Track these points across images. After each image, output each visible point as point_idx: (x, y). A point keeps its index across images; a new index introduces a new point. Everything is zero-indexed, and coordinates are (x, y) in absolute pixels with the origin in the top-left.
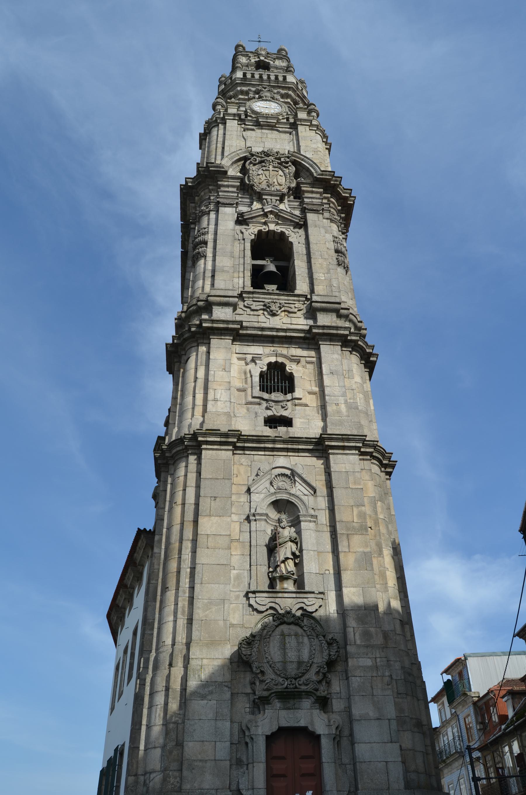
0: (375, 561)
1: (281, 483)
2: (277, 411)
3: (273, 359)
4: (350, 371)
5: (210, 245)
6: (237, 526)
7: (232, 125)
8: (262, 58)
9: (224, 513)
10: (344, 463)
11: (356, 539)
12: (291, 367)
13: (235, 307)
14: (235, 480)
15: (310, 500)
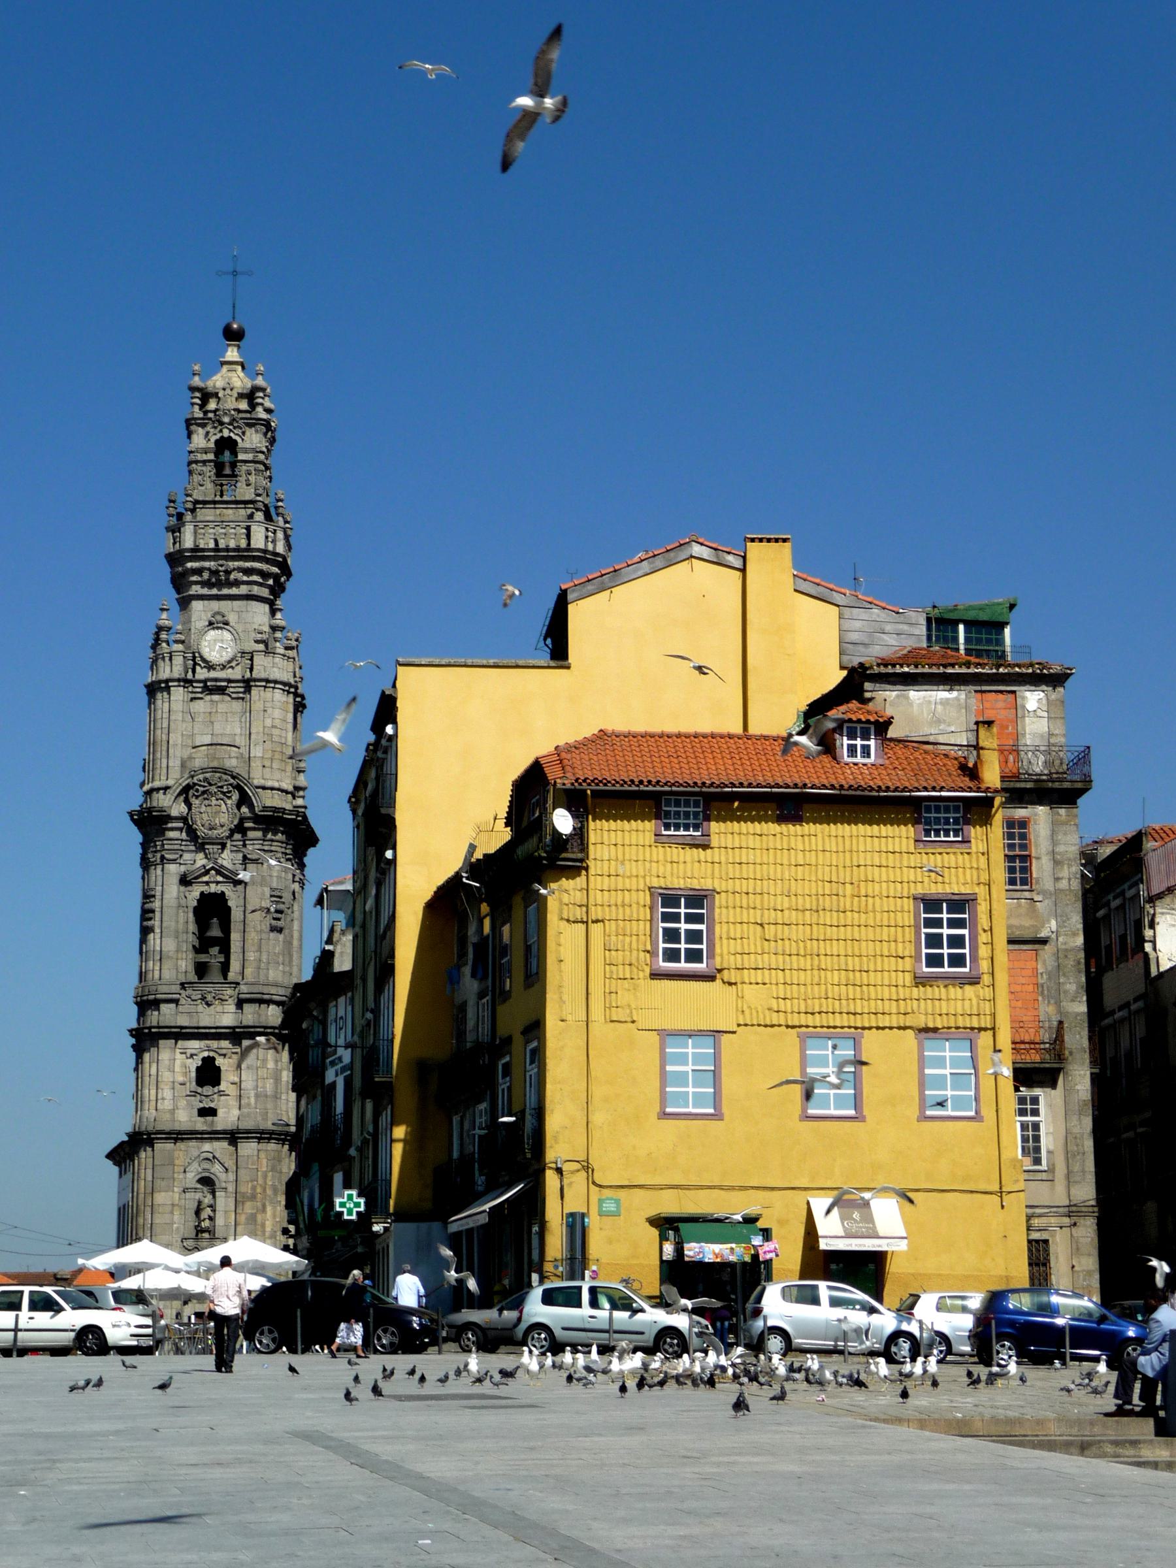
0: (259, 1217)
1: (206, 1165)
2: (207, 1104)
3: (206, 1054)
4: (265, 1061)
5: (158, 915)
6: (177, 1196)
7: (178, 693)
8: (226, 433)
9: (169, 1189)
10: (248, 1148)
11: (248, 1204)
12: (219, 1061)
13: (176, 1002)
14: (177, 1162)
15: (223, 1176)
